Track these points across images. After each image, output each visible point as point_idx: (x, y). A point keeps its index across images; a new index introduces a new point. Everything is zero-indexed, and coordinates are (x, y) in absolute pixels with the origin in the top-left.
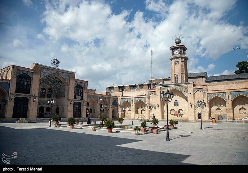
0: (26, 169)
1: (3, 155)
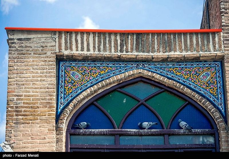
0: (24, 156)
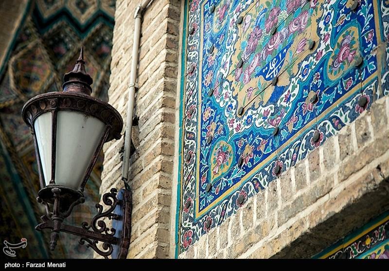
0: (40, 265)
1: (6, 242)
